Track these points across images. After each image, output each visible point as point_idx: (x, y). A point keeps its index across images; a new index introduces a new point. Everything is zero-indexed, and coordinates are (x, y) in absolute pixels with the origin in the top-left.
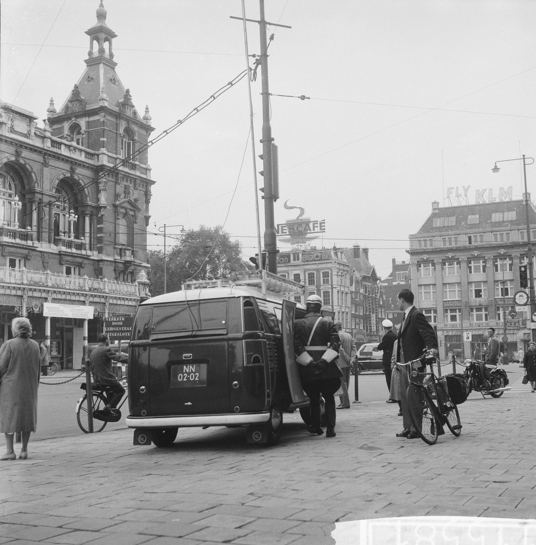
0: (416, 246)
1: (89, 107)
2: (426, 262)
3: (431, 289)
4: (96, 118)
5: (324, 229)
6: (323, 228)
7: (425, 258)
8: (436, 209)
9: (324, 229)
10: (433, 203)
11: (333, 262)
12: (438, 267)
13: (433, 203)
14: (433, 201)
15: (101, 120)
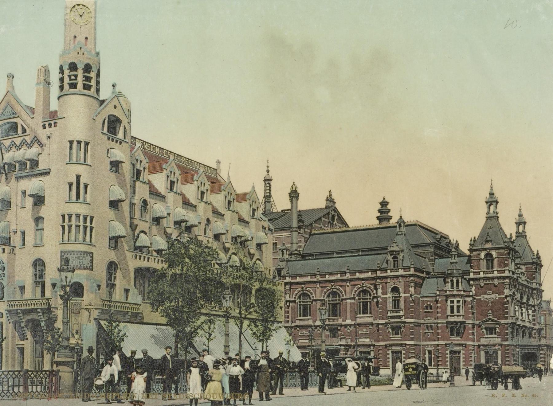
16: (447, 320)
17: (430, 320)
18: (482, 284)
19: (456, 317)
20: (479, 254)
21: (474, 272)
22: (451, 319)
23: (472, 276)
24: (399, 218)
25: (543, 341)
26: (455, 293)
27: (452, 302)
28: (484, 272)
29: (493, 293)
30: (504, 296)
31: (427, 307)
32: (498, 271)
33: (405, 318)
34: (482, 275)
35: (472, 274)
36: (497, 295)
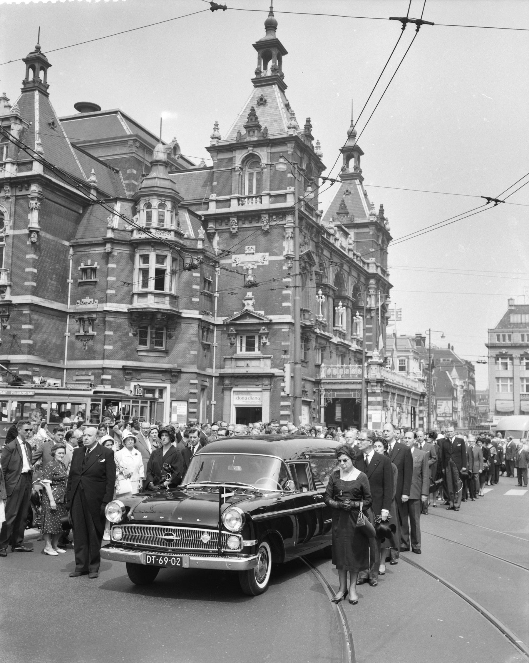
0: (495, 341)
1: (358, 221)
2: (503, 356)
3: (509, 383)
4: (366, 230)
5: (400, 318)
6: (399, 316)
7: (504, 352)
8: (512, 306)
9: (400, 318)
10: (509, 300)
11: (411, 350)
12: (517, 362)
13: (509, 300)
14: (509, 298)
15: (371, 233)
16: (130, 306)
17: (89, 304)
18: (234, 228)
19: (150, 297)
20: (231, 160)
21: (217, 201)
22: (138, 304)
23: (213, 209)
24: (33, 49)
25: (375, 373)
26: (155, 234)
27: (145, 259)
28: (239, 199)
29: (257, 252)
30: (281, 258)
31: (84, 270)
32: (271, 196)
33: (12, 294)
34: (235, 207)
35: (212, 205)
36: (267, 254)
